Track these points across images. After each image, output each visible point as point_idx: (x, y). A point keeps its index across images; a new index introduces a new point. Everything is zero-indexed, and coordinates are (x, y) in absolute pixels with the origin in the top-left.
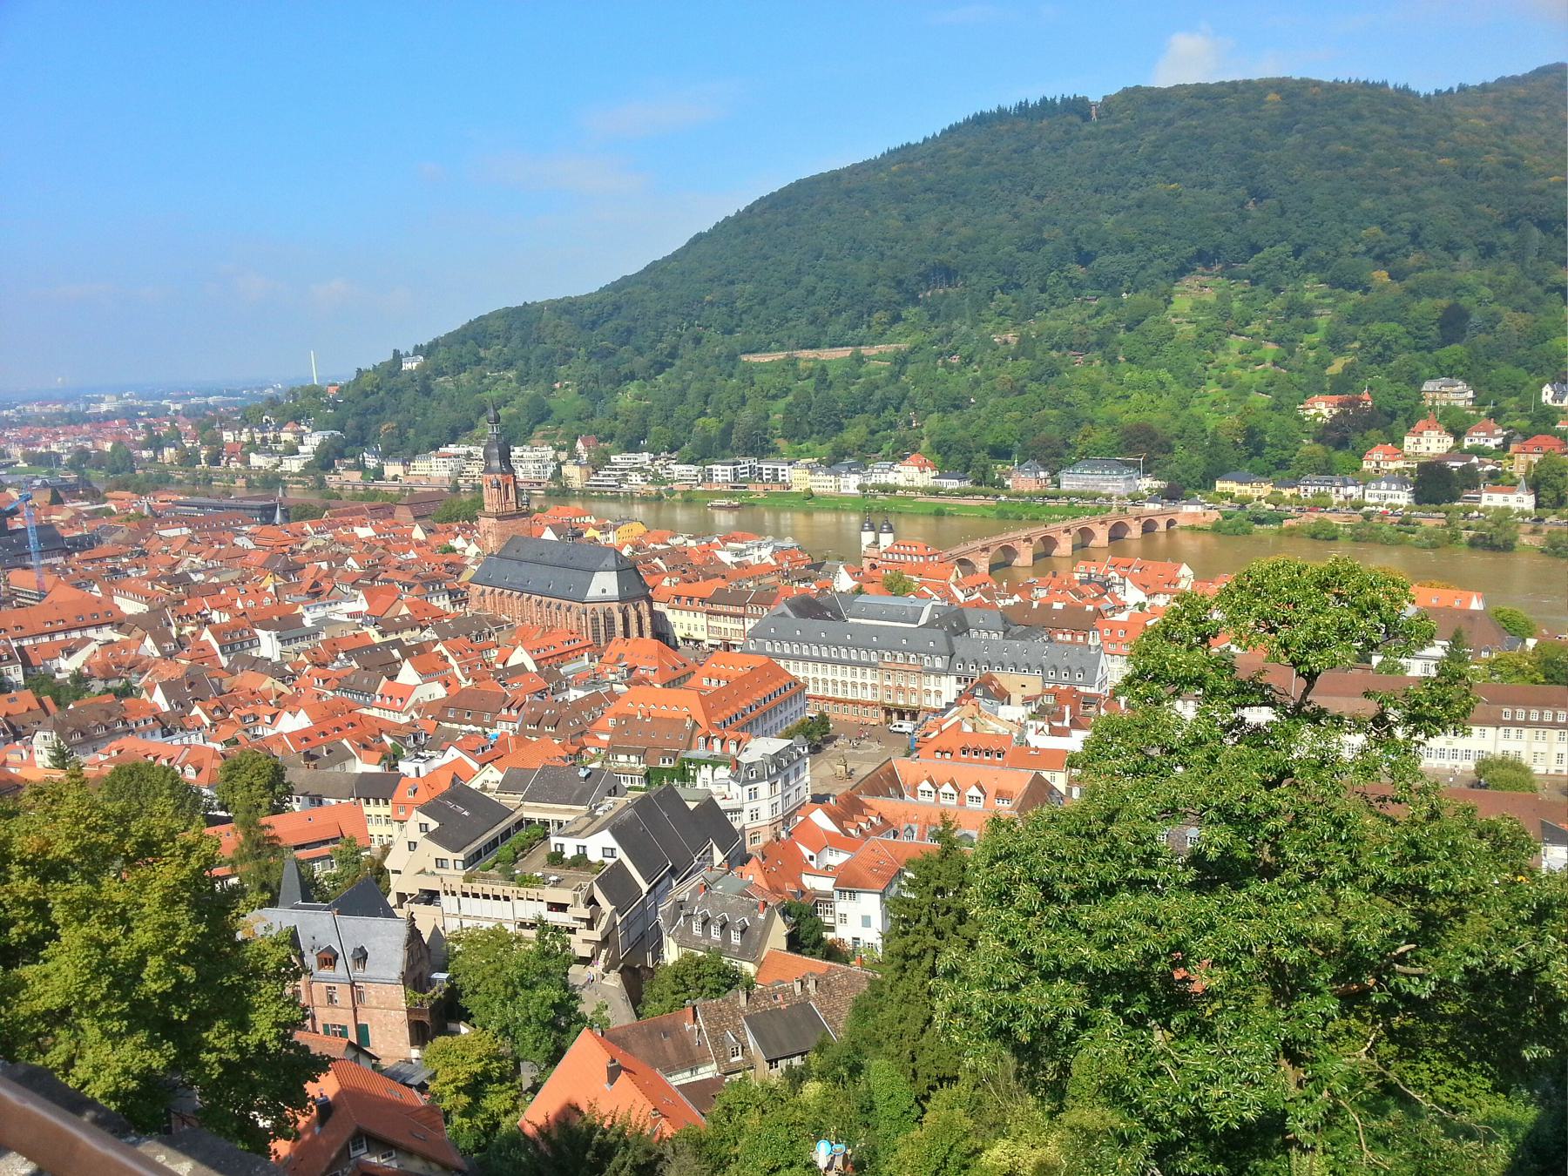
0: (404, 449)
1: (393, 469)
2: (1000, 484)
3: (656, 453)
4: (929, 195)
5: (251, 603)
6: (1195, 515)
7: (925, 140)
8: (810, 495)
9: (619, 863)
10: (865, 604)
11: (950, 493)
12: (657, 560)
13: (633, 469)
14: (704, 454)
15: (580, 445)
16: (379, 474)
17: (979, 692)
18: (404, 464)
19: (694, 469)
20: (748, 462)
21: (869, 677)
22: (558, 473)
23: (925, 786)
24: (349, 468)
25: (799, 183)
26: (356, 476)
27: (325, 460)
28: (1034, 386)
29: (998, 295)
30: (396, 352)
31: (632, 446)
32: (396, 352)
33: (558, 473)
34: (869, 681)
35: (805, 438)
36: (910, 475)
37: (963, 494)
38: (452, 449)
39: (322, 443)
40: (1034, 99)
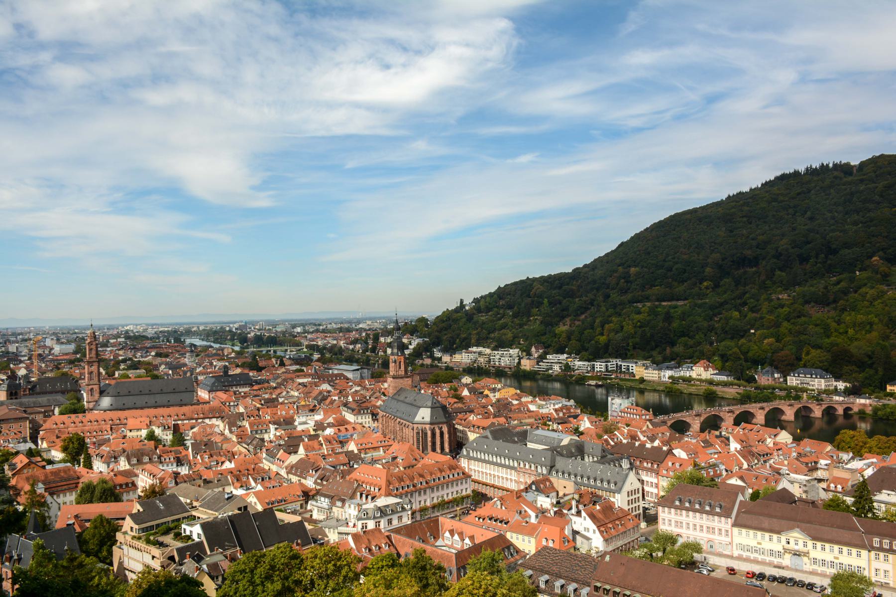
0: (451, 350)
1: (446, 358)
2: (751, 380)
3: (570, 353)
4: (745, 219)
5: (284, 413)
6: (864, 405)
7: (751, 190)
8: (642, 380)
9: (202, 542)
10: (536, 435)
11: (719, 384)
12: (490, 407)
13: (555, 362)
14: (594, 356)
15: (533, 349)
16: (440, 359)
17: (534, 487)
18: (451, 356)
19: (586, 363)
20: (613, 363)
21: (513, 475)
22: (519, 363)
23: (447, 534)
24: (428, 357)
25: (677, 215)
26: (428, 361)
27: (418, 353)
28: (785, 324)
29: (778, 273)
30: (462, 301)
31: (561, 351)
32: (462, 301)
33: (519, 363)
34: (513, 478)
35: (652, 349)
36: (700, 372)
37: (726, 384)
38: (474, 349)
39: (418, 344)
40: (816, 165)
